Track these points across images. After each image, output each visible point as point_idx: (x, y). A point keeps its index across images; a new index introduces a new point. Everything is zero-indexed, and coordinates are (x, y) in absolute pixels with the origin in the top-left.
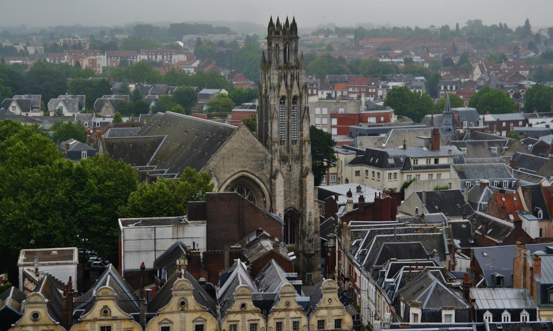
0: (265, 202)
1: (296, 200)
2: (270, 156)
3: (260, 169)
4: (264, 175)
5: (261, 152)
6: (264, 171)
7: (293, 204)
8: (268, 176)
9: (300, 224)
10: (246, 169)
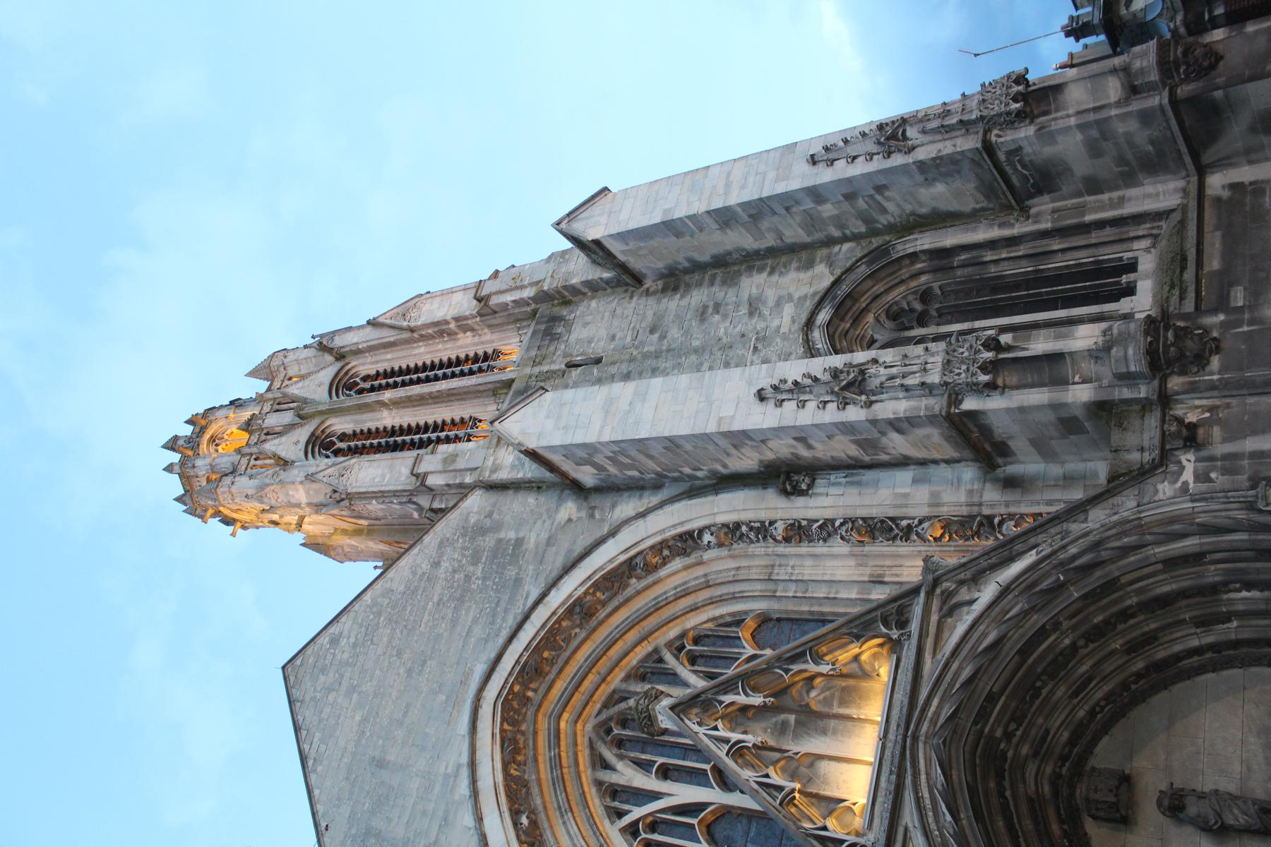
0: (733, 532)
1: (771, 295)
3: (511, 572)
4: (550, 542)
5: (436, 564)
7: (788, 310)
8: (570, 508)
9: (950, 238)
10: (480, 669)
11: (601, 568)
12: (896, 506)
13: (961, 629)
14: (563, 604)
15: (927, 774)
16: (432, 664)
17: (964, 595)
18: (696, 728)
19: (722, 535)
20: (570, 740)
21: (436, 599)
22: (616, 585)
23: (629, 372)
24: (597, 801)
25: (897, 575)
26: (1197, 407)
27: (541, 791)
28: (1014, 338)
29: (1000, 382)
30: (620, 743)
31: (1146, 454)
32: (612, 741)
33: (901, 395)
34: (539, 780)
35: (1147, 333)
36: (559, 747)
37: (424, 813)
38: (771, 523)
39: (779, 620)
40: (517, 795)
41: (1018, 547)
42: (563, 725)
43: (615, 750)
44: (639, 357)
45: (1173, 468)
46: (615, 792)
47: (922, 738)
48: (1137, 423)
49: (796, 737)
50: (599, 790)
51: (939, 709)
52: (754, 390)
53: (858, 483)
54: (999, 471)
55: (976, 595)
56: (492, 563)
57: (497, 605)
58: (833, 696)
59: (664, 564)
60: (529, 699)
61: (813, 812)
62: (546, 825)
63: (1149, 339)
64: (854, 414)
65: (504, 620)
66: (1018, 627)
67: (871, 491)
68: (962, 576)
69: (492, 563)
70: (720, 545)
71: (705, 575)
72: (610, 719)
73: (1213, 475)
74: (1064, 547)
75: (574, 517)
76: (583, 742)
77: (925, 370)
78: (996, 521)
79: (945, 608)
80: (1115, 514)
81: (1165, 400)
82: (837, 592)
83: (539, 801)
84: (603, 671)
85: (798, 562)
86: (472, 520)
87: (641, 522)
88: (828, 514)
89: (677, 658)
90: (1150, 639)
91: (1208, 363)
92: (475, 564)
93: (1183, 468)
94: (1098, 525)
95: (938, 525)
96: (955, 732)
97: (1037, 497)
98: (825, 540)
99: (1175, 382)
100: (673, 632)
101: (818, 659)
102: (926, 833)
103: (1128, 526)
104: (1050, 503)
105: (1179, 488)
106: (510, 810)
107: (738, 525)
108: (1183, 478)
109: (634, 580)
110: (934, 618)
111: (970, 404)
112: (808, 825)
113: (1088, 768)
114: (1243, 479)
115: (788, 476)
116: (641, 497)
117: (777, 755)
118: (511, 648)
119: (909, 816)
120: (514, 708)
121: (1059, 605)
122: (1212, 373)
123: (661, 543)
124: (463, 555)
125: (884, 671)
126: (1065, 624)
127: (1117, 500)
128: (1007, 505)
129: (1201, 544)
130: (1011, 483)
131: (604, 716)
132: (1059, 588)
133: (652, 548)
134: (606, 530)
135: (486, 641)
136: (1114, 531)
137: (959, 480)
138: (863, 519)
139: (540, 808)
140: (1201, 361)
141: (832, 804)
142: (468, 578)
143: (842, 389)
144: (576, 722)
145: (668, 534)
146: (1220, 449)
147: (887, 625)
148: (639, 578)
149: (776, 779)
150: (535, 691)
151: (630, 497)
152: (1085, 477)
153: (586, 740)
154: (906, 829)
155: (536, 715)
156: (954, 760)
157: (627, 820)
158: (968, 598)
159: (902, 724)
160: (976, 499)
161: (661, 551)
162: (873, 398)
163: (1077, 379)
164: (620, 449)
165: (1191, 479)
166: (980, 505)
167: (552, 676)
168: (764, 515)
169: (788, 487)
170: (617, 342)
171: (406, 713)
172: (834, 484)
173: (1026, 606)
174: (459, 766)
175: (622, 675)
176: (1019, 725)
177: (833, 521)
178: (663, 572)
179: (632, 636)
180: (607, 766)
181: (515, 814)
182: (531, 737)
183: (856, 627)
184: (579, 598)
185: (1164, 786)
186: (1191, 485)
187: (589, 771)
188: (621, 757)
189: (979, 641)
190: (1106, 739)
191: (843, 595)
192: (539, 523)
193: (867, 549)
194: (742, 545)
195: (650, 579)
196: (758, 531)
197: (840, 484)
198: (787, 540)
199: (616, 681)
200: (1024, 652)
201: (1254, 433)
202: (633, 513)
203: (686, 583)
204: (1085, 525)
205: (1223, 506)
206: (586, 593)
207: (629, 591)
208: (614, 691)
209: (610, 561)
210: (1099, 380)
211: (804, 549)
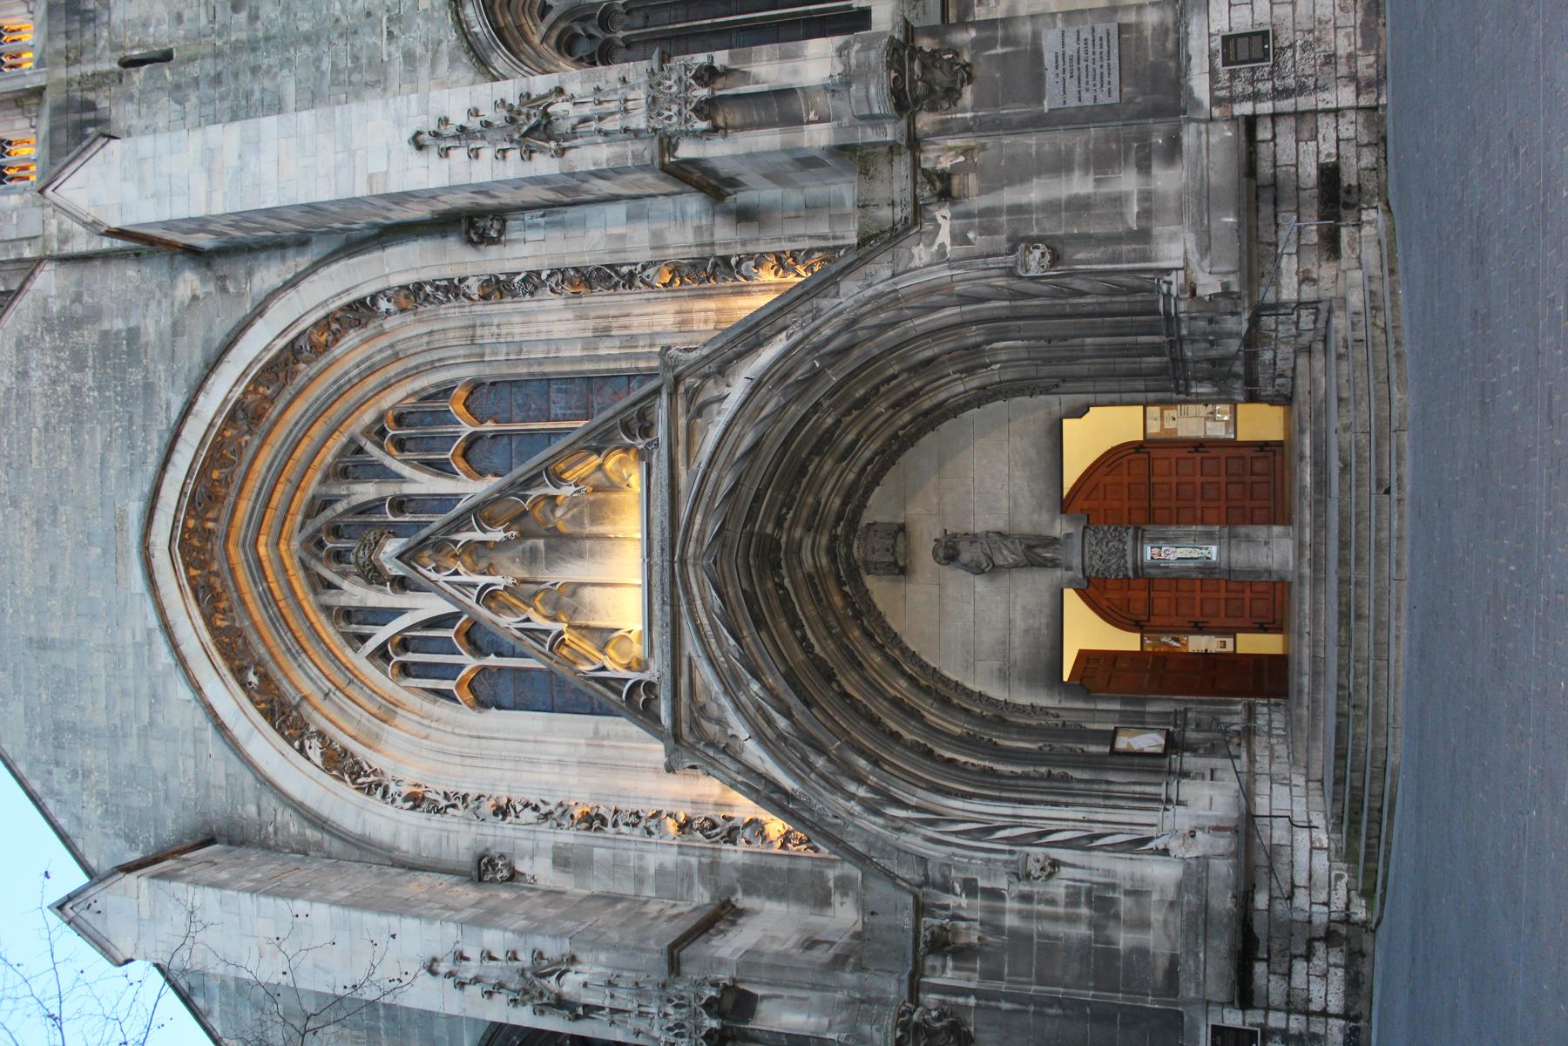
0: (414, 295)
2: (47, 280)
3: (135, 376)
4: (176, 330)
5: (23, 375)
6: (150, 332)
8: (189, 282)
10: (135, 509)
11: (256, 360)
12: (612, 252)
13: (714, 433)
14: (219, 412)
15: (703, 599)
16: (66, 510)
17: (711, 390)
18: (433, 576)
19: (402, 300)
20: (276, 566)
21: (40, 422)
22: (282, 375)
23: (219, 75)
24: (331, 630)
25: (625, 327)
26: (950, 149)
27: (261, 638)
28: (731, 57)
29: (720, 121)
30: (338, 556)
31: (898, 210)
32: (328, 556)
33: (600, 139)
34: (254, 624)
35: (889, 66)
36: (266, 578)
37: (124, 693)
38: (461, 280)
39: (493, 384)
40: (234, 650)
41: (765, 331)
42: (262, 550)
43: (335, 566)
44: (227, 49)
45: (928, 227)
46: (348, 614)
47: (690, 561)
48: (885, 169)
49: (550, 564)
50: (329, 616)
51: (705, 526)
52: (408, 134)
53: (561, 224)
54: (729, 200)
55: (726, 390)
56: (104, 366)
57: (131, 423)
58: (581, 512)
59: (337, 340)
60: (210, 532)
61: (587, 647)
62: (280, 675)
63: (893, 75)
64: (544, 165)
65: (145, 440)
66: (776, 422)
67: (578, 233)
68: (706, 369)
69: (104, 366)
70: (403, 310)
71: (392, 346)
72: (319, 531)
73: (971, 235)
74: (817, 329)
75: (199, 292)
76: (292, 564)
77: (626, 110)
78: (733, 261)
79: (693, 408)
80: (870, 286)
81: (914, 143)
82: (558, 350)
83: (262, 650)
84: (294, 477)
85: (504, 320)
86: (55, 307)
87: (292, 293)
88: (531, 265)
89: (381, 447)
90: (915, 394)
91: (960, 95)
92: (81, 368)
93: (939, 226)
94: (851, 302)
95: (666, 270)
96: (724, 545)
97: (777, 232)
98: (532, 294)
99: (925, 121)
100: (368, 416)
101: (557, 480)
102: (712, 661)
103: (884, 300)
104: (792, 239)
105: (933, 255)
106: (232, 670)
107: (419, 286)
108: (939, 240)
109: (302, 366)
110: (682, 422)
111: (686, 150)
112: (585, 667)
113: (864, 522)
114: (1001, 241)
115: (474, 222)
116: (283, 258)
117: (534, 588)
118: (168, 477)
119: (691, 646)
120: (195, 547)
121: (818, 393)
122: (964, 110)
123: (327, 316)
124: (58, 358)
125: (635, 478)
126: (825, 405)
127: (870, 268)
128: (744, 243)
129: (962, 313)
130: (745, 215)
131: (309, 529)
132: (814, 376)
133: (316, 325)
134: (248, 307)
135: (131, 472)
136: (869, 307)
137: (684, 214)
138: (575, 269)
139: (267, 657)
140: (952, 94)
141: (603, 637)
142: (77, 390)
143: (524, 136)
144: (278, 544)
145: (333, 306)
146: (978, 202)
147: (631, 436)
148: (308, 362)
149: (539, 622)
150: (215, 520)
151: (268, 259)
152: (829, 205)
153: (296, 560)
154: (690, 659)
155: (226, 549)
156: (727, 575)
157: (372, 645)
158: (716, 394)
159: (667, 549)
160: (706, 239)
161: (329, 325)
162: (566, 144)
163: (812, 116)
164: (239, 219)
165: (948, 242)
166: (712, 244)
167: (231, 499)
168: (449, 272)
169: (475, 238)
170: (187, 25)
171: (53, 578)
172: (531, 226)
173: (783, 401)
174: (150, 632)
175: (318, 476)
176: (790, 509)
177: (538, 273)
178: (337, 351)
179: (318, 430)
180: (330, 586)
181: (239, 673)
182: (228, 576)
183: (594, 439)
184: (238, 401)
185: (938, 534)
186: (949, 248)
187: (311, 597)
188: (344, 575)
189: (736, 445)
190: (877, 489)
191: (565, 353)
192: (153, 304)
193: (584, 300)
194: (429, 307)
195: (323, 361)
196: (446, 290)
197: (537, 226)
198: (485, 297)
199: (312, 484)
200: (786, 444)
201: (1011, 183)
202: (278, 282)
203: (368, 358)
204: (837, 301)
205: (981, 274)
206: (245, 393)
207: (300, 380)
208: (314, 497)
209: (267, 349)
210: (838, 118)
211: (508, 306)
